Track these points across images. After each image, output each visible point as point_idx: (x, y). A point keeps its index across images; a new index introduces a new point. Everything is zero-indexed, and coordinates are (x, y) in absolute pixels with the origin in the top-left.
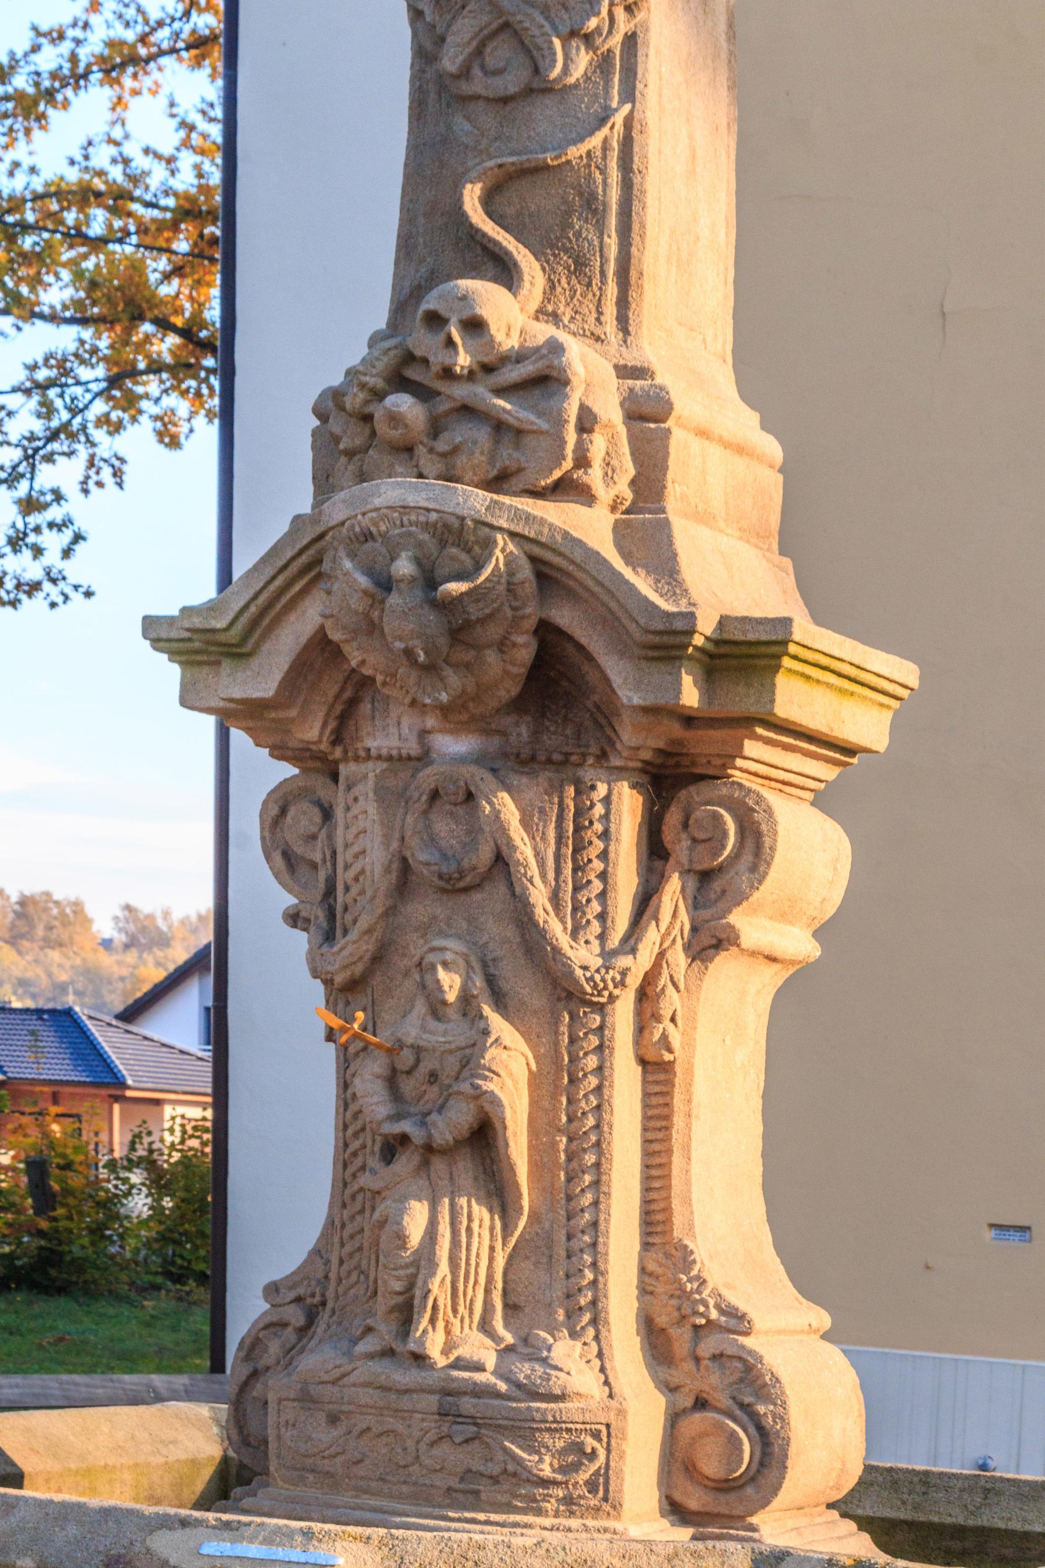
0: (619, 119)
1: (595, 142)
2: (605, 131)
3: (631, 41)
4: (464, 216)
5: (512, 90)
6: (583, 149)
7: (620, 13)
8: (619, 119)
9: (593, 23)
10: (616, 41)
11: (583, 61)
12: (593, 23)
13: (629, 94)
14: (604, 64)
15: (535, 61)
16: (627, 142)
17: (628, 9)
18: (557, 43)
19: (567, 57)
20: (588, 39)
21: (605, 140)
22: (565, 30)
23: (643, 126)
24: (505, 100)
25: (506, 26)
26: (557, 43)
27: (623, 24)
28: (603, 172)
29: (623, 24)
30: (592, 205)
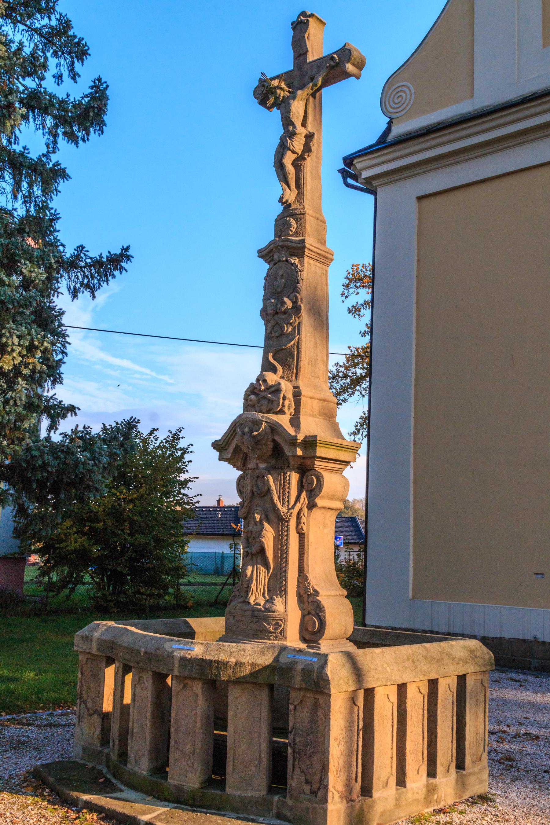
0: (296, 339)
1: (292, 343)
2: (294, 341)
3: (299, 324)
4: (268, 359)
5: (278, 335)
6: (290, 345)
7: (297, 319)
8: (296, 339)
9: (291, 321)
10: (297, 323)
11: (290, 328)
12: (291, 321)
13: (299, 334)
14: (294, 329)
15: (282, 328)
16: (298, 343)
17: (298, 318)
18: (285, 325)
19: (287, 328)
20: (291, 324)
21: (294, 343)
22: (286, 323)
23: (301, 339)
24: (277, 337)
25: (277, 323)
26: (285, 325)
27: (297, 321)
28: (294, 349)
29: (297, 321)
30: (292, 355)
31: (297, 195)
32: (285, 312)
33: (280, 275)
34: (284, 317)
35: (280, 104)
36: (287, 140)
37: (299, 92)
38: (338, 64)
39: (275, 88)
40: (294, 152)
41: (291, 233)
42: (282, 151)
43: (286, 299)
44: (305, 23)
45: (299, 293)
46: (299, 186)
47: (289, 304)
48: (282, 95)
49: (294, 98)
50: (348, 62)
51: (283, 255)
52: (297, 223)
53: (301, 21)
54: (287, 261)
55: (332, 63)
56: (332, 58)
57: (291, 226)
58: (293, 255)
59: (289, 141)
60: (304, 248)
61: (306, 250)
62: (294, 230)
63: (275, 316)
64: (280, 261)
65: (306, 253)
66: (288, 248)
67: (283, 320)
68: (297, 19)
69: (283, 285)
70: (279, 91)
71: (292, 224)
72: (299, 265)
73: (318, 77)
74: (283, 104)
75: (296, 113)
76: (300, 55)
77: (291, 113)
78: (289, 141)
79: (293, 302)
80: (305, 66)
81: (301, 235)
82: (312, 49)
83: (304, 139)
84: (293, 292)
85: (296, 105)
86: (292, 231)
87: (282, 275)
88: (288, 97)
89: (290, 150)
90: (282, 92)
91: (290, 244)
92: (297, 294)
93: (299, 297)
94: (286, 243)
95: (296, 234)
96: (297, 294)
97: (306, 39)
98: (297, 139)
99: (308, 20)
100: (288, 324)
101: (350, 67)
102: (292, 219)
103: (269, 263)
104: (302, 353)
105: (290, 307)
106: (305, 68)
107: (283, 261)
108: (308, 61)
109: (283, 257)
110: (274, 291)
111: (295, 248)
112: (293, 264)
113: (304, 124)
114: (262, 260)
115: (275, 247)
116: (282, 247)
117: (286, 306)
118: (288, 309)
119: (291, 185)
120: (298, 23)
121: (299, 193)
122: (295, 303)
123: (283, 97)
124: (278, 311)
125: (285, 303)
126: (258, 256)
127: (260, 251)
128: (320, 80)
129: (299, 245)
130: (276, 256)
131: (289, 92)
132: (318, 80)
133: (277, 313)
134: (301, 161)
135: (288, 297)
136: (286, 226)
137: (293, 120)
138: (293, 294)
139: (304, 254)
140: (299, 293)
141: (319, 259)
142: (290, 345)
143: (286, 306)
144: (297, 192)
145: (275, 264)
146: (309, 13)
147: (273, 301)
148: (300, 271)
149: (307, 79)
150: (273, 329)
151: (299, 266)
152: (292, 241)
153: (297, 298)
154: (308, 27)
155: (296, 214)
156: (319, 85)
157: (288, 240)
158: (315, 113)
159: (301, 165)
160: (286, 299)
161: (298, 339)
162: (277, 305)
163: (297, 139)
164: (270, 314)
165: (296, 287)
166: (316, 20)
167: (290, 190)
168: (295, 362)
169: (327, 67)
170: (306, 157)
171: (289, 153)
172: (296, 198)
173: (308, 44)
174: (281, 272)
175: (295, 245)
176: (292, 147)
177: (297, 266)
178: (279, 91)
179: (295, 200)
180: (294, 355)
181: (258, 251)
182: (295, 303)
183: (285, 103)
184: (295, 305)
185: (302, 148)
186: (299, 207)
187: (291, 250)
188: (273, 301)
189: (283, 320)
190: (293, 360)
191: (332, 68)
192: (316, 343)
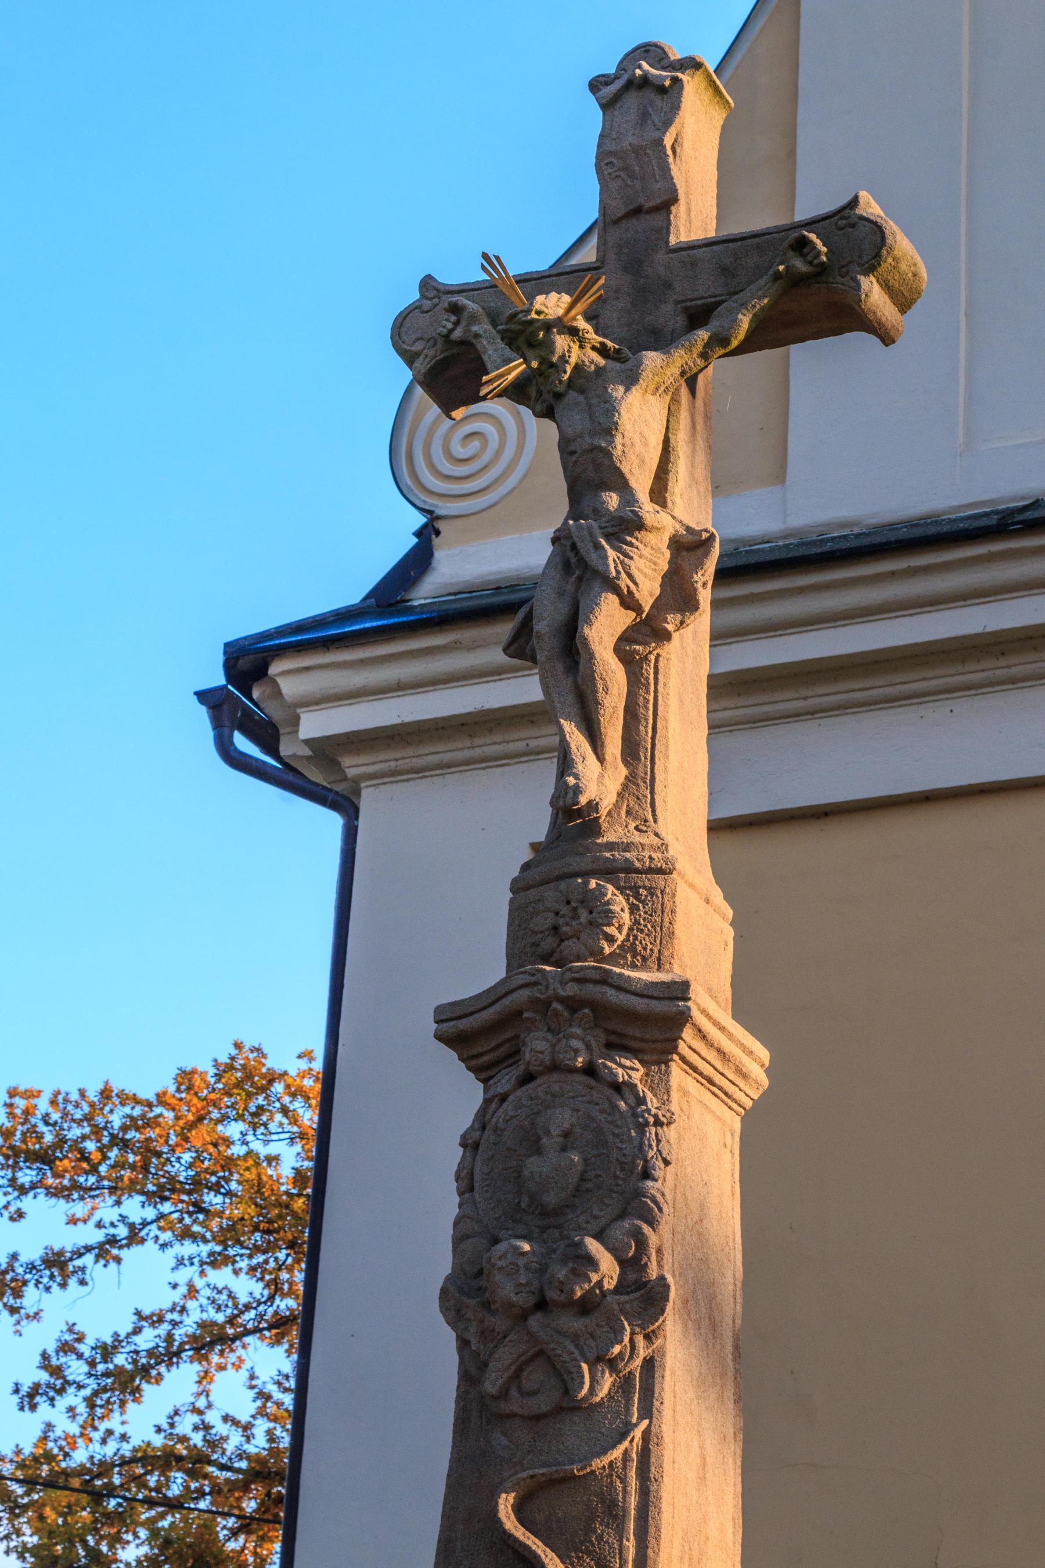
0: (638, 1433)
1: (617, 1453)
2: (626, 1444)
3: (650, 1365)
4: (499, 1522)
5: (545, 1408)
6: (606, 1460)
7: (640, 1341)
8: (638, 1433)
9: (617, 1349)
10: (638, 1362)
11: (607, 1382)
12: (617, 1349)
13: (647, 1412)
14: (625, 1385)
15: (567, 1381)
16: (645, 1453)
17: (648, 1337)
18: (585, 1366)
19: (594, 1381)
20: (612, 1364)
21: (626, 1452)
22: (592, 1356)
23: (660, 1438)
24: (538, 1418)
25: (541, 1353)
26: (585, 1366)
27: (642, 1352)
28: (624, 1481)
29: (642, 1352)
30: (614, 1513)
31: (625, 787)
32: (586, 1306)
33: (555, 1132)
34: (575, 1324)
35: (558, 396)
36: (598, 547)
37: (652, 359)
38: (822, 270)
39: (548, 326)
40: (628, 602)
41: (607, 950)
42: (570, 588)
43: (593, 1246)
44: (662, 90)
45: (652, 1223)
46: (631, 751)
47: (608, 1269)
48: (573, 360)
49: (631, 380)
50: (870, 269)
51: (575, 1043)
52: (633, 909)
53: (645, 82)
54: (590, 1070)
55: (800, 265)
56: (802, 245)
57: (608, 916)
58: (617, 1045)
59: (611, 554)
60: (683, 1018)
61: (687, 1033)
62: (621, 938)
63: (535, 1322)
64: (555, 1067)
65: (682, 1047)
66: (601, 1012)
67: (575, 1338)
68: (622, 67)
69: (573, 1180)
70: (561, 342)
71: (616, 908)
72: (649, 1095)
73: (733, 312)
74: (572, 395)
75: (637, 440)
76: (637, 211)
77: (618, 440)
78: (611, 554)
79: (622, 1262)
80: (660, 257)
81: (652, 963)
82: (687, 194)
83: (668, 554)
84: (622, 1215)
85: (636, 410)
86: (611, 939)
87: (566, 1135)
88: (599, 371)
89: (616, 590)
90: (575, 347)
91: (613, 996)
92: (646, 1229)
93: (653, 1239)
94: (593, 991)
95: (630, 951)
96: (646, 1229)
97: (669, 152)
98: (646, 551)
99: (676, 81)
100: (602, 1360)
101: (874, 294)
102: (610, 888)
103: (483, 1072)
104: (665, 1506)
105: (609, 1285)
106: (659, 264)
107: (572, 1070)
108: (673, 240)
109: (576, 1051)
110: (525, 1202)
111: (631, 1016)
112: (618, 1088)
113: (659, 493)
114: (455, 1055)
115: (534, 1002)
116: (573, 1005)
117: (595, 1278)
118: (604, 1294)
119: (608, 741)
120: (630, 84)
121: (631, 779)
122: (632, 1264)
123: (578, 368)
124: (552, 1295)
125: (592, 1263)
126: (439, 1037)
127: (446, 1014)
128: (745, 321)
129: (658, 1007)
130: (537, 1045)
131: (602, 350)
132: (735, 322)
133: (542, 1305)
134: (646, 644)
135: (599, 1236)
136: (584, 916)
137: (625, 468)
138: (626, 1224)
139: (675, 1049)
140: (652, 1223)
141: (717, 1078)
142: (606, 1460)
143: (595, 1278)
144: (624, 771)
145: (528, 1078)
146: (676, 53)
147: (526, 1247)
148: (658, 1123)
149: (667, 314)
150: (517, 1375)
151: (652, 1102)
152: (623, 986)
153: (642, 1243)
154: (676, 107)
155: (629, 869)
156: (735, 343)
157: (605, 979)
158: (694, 451)
159: (646, 658)
160: (593, 1246)
161: (646, 1435)
162: (543, 1269)
163: (646, 551)
164: (511, 1305)
165: (641, 1193)
166: (703, 84)
167: (601, 759)
168: (631, 1546)
169: (777, 276)
170: (670, 627)
171: (609, 603)
172: (620, 795)
173: (675, 172)
174: (562, 1118)
175: (639, 1004)
176: (624, 582)
177: (642, 1101)
178: (561, 342)
179: (617, 806)
180: (625, 1511)
181: (439, 1010)
182: (632, 1264)
183: (582, 391)
184: (632, 1276)
185: (658, 592)
186: (637, 838)
187: (612, 1026)
188: (526, 1247)
189: (575, 1338)
190: (621, 1534)
191: (794, 282)
192: (704, 1465)
